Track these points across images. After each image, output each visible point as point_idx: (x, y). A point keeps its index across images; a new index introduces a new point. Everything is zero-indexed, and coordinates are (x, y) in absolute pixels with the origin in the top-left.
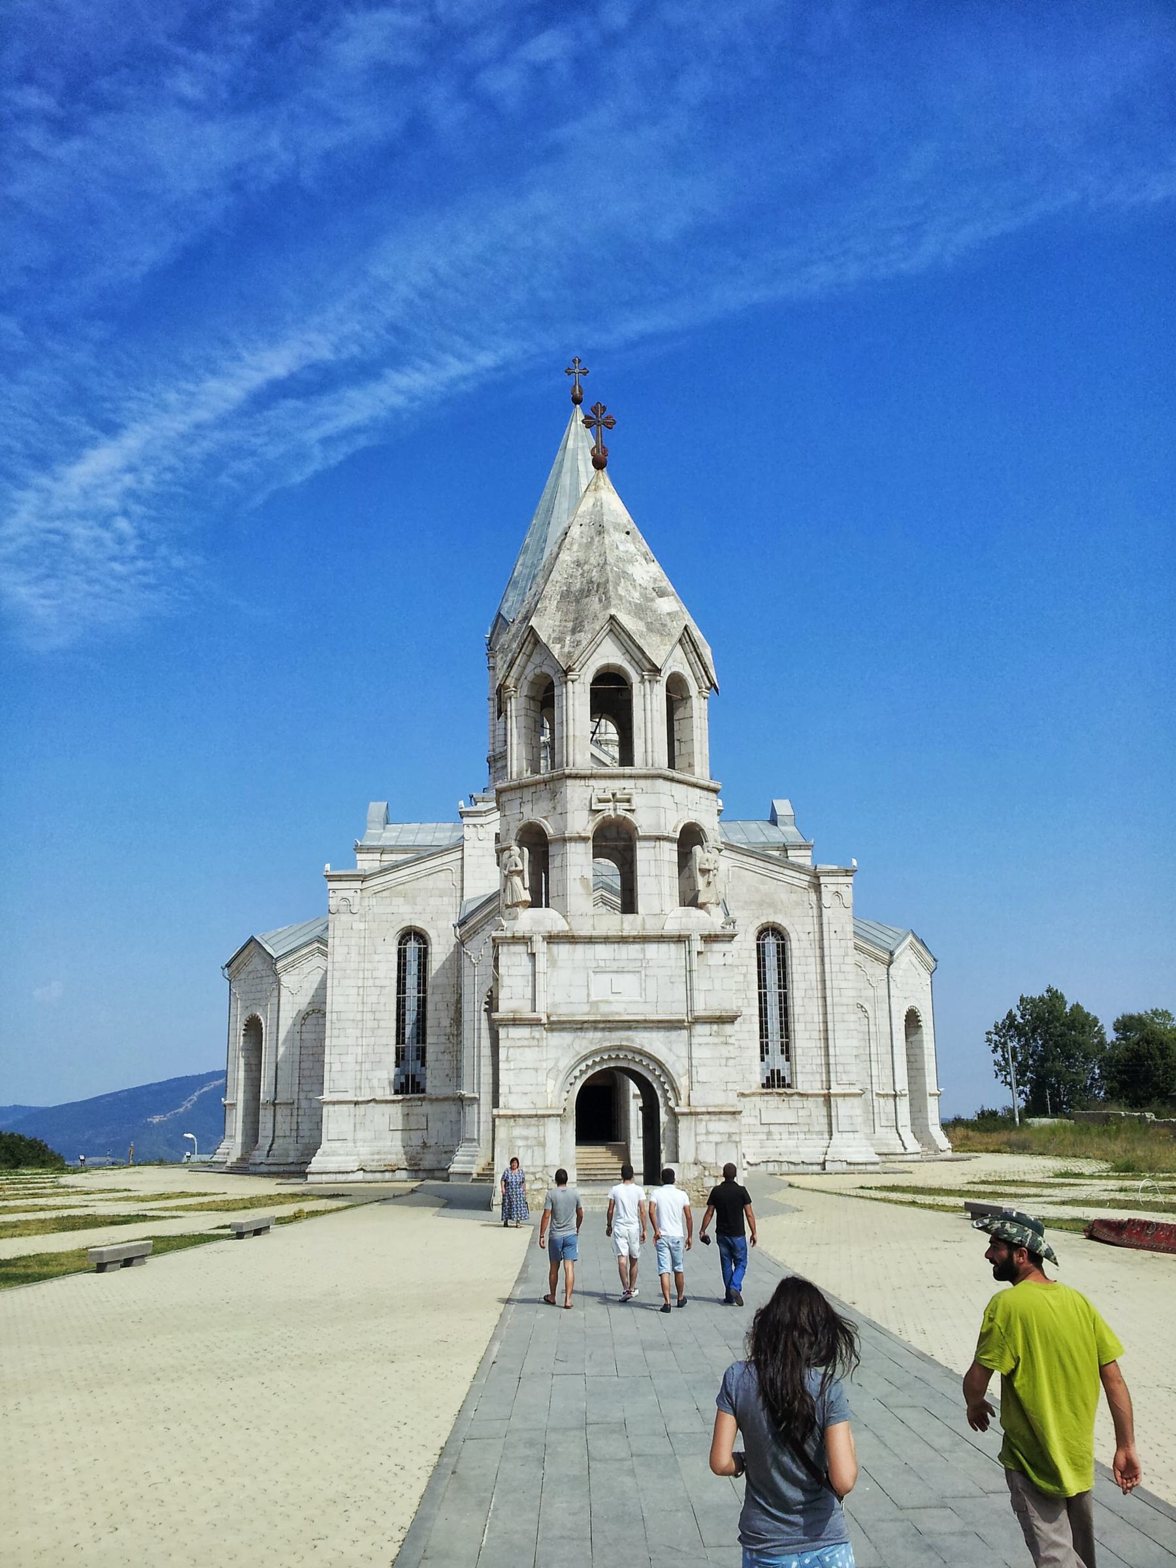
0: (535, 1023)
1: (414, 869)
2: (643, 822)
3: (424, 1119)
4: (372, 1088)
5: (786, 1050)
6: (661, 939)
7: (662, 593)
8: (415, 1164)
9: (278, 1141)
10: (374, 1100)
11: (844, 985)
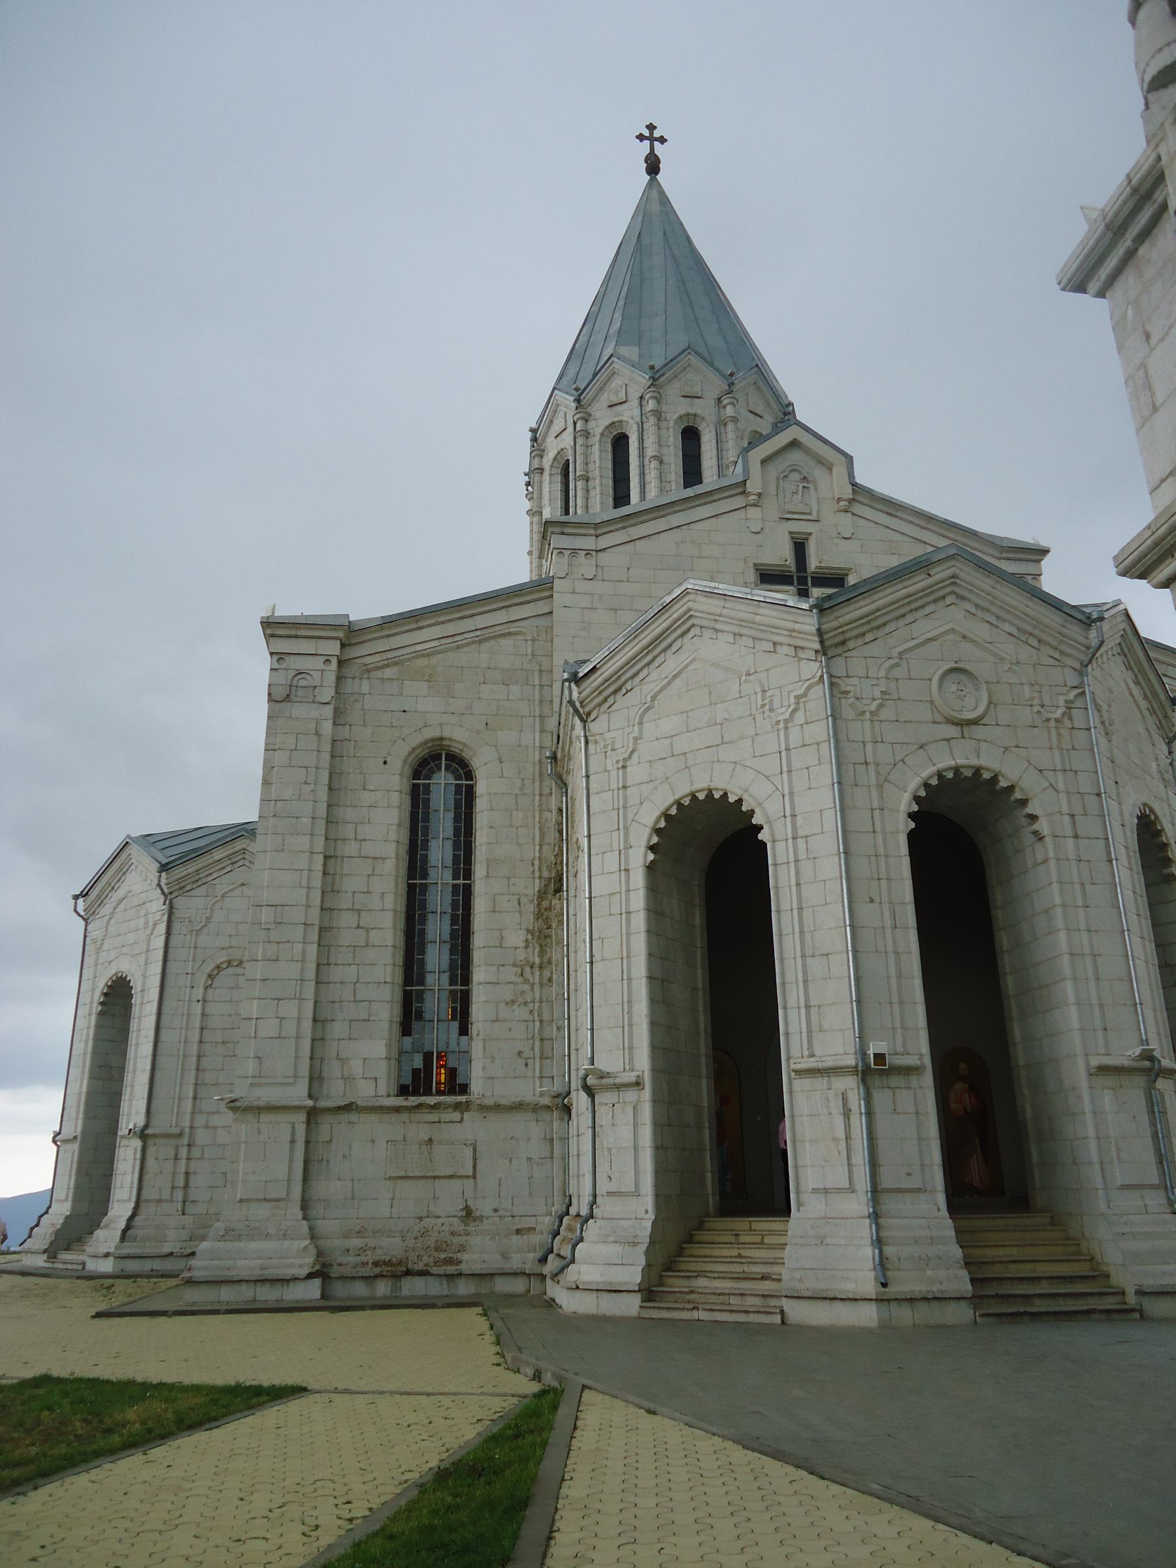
1: (451, 629)
3: (469, 1152)
4: (348, 1079)
8: (449, 1261)
9: (146, 1211)
10: (349, 1108)
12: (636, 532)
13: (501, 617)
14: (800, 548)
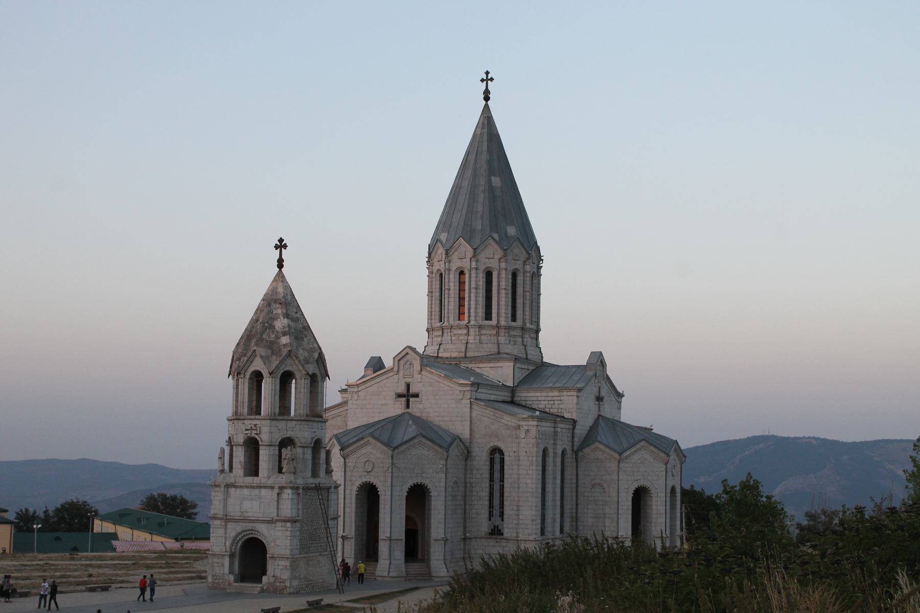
0: (221, 519)
2: (264, 437)
5: (502, 515)
6: (266, 487)
7: (284, 334)
11: (529, 481)
12: (367, 385)
13: (338, 411)
14: (408, 386)
